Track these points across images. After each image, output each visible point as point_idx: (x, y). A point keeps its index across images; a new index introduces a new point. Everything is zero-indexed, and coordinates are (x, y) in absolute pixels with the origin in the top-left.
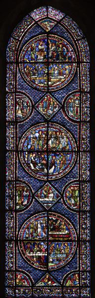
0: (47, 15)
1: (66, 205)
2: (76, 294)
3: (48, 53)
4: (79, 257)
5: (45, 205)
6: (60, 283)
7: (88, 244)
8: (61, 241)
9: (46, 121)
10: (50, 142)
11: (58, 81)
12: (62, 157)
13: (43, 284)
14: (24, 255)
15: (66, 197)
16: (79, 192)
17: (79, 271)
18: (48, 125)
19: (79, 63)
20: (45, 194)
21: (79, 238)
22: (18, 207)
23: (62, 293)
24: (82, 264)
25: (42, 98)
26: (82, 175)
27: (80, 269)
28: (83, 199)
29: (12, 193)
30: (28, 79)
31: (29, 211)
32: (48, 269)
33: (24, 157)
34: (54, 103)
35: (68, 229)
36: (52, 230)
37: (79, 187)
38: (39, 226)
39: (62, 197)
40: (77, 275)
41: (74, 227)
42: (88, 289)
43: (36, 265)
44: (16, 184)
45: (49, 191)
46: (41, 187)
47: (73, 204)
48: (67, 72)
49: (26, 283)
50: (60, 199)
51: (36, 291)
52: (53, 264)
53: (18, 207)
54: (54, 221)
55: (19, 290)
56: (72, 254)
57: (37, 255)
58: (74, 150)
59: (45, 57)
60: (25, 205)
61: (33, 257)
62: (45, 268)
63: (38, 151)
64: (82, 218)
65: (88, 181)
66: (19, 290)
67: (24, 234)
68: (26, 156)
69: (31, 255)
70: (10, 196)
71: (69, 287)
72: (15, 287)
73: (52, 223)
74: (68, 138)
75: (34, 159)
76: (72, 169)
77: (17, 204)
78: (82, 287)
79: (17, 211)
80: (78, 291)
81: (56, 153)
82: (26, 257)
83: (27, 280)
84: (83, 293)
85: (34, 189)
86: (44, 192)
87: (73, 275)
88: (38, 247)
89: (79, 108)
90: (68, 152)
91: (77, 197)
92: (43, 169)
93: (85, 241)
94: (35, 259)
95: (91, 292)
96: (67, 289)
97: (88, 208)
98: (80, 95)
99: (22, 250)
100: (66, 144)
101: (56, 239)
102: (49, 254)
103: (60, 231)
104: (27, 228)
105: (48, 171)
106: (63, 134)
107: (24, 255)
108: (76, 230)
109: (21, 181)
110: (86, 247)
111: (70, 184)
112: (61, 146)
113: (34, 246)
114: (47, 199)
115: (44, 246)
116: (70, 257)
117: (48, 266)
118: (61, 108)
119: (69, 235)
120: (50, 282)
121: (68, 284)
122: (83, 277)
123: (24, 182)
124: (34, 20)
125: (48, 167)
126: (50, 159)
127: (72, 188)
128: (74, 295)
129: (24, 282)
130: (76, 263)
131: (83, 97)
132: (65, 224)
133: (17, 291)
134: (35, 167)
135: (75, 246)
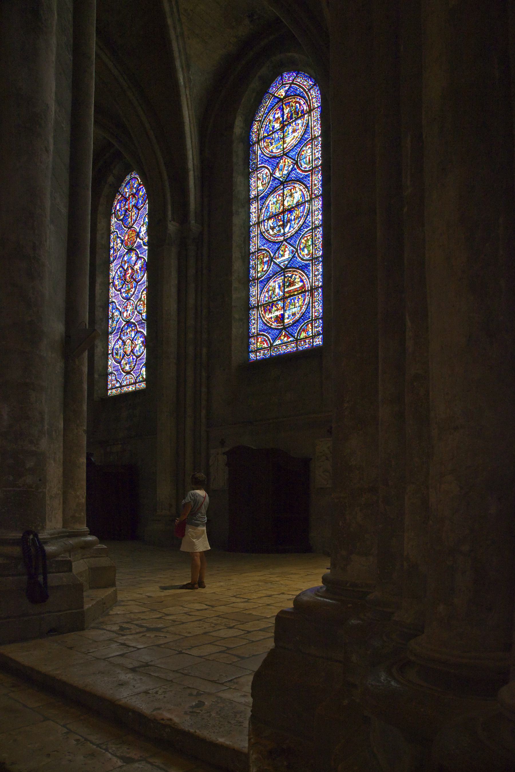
0: (283, 82)
1: (300, 257)
2: (309, 344)
3: (283, 119)
4: (312, 306)
5: (282, 264)
6: (294, 337)
7: (320, 290)
8: (296, 295)
9: (282, 183)
10: (285, 202)
11: (293, 139)
12: (296, 212)
13: (280, 342)
14: (264, 318)
15: (300, 249)
16: (312, 239)
17: (312, 320)
18: (283, 186)
19: (310, 111)
20: (282, 253)
21: (311, 287)
22: (259, 275)
23: (297, 347)
24: (315, 312)
25: (278, 164)
26: (314, 222)
27: (312, 318)
28: (316, 246)
29: (255, 263)
30: (268, 152)
31: (269, 275)
32: (283, 325)
33: (264, 226)
34: (288, 162)
35: (302, 281)
36: (288, 286)
37: (312, 235)
38: (277, 286)
39: (297, 251)
40: (310, 325)
41: (307, 277)
42: (321, 336)
43: (274, 325)
44: (258, 253)
45: (285, 249)
46: (278, 248)
47: (306, 255)
48: (300, 126)
49: (265, 344)
50: (295, 254)
51: (274, 350)
52: (289, 320)
53: (259, 275)
54: (290, 277)
55: (260, 352)
56: (306, 305)
57: (274, 315)
58: (306, 199)
59: (281, 123)
60: (265, 271)
61: (271, 318)
62: (281, 326)
63: (275, 215)
64: (315, 265)
65: (321, 226)
66: (260, 352)
67: (264, 298)
68: (266, 224)
69: (270, 316)
70: (253, 266)
71: (303, 338)
72: (257, 350)
73: (288, 280)
74: (301, 190)
75: (272, 224)
76: (306, 220)
77: (258, 272)
78: (315, 335)
79: (258, 279)
80: (311, 341)
81: (290, 210)
82: (266, 320)
83: (266, 341)
84: (316, 342)
85: (272, 252)
86: (281, 251)
87: (306, 326)
88: (276, 307)
89: (311, 157)
90: (303, 204)
91: (310, 245)
92: (280, 231)
93: (317, 288)
94: (273, 319)
95: (323, 340)
96: (301, 342)
97: (321, 253)
98: (312, 143)
99: (262, 314)
100: (300, 197)
101: (291, 295)
102: (285, 311)
103: (295, 285)
104: (267, 292)
105: (284, 231)
106: (297, 188)
107: (264, 318)
108: (309, 279)
109: (262, 249)
110: (319, 294)
111: (303, 235)
112: (295, 202)
113: (272, 307)
114: (283, 258)
115: (280, 304)
116: (304, 308)
117: (284, 322)
118: (295, 164)
119: (304, 286)
120: (286, 338)
121: (302, 337)
122: (316, 325)
123: (265, 250)
124: (270, 94)
125: (284, 226)
126: (285, 218)
127: (306, 239)
128: (307, 346)
129: (264, 344)
130: (309, 313)
131: (314, 142)
132: (299, 277)
133: (258, 354)
134: (273, 231)
135: (308, 295)
